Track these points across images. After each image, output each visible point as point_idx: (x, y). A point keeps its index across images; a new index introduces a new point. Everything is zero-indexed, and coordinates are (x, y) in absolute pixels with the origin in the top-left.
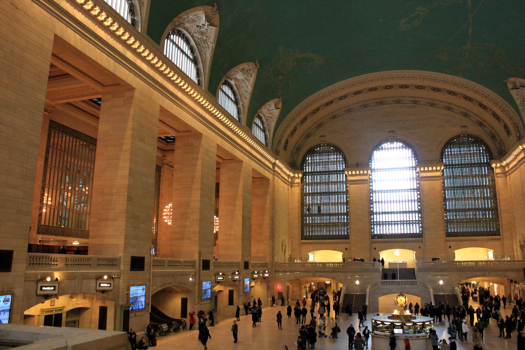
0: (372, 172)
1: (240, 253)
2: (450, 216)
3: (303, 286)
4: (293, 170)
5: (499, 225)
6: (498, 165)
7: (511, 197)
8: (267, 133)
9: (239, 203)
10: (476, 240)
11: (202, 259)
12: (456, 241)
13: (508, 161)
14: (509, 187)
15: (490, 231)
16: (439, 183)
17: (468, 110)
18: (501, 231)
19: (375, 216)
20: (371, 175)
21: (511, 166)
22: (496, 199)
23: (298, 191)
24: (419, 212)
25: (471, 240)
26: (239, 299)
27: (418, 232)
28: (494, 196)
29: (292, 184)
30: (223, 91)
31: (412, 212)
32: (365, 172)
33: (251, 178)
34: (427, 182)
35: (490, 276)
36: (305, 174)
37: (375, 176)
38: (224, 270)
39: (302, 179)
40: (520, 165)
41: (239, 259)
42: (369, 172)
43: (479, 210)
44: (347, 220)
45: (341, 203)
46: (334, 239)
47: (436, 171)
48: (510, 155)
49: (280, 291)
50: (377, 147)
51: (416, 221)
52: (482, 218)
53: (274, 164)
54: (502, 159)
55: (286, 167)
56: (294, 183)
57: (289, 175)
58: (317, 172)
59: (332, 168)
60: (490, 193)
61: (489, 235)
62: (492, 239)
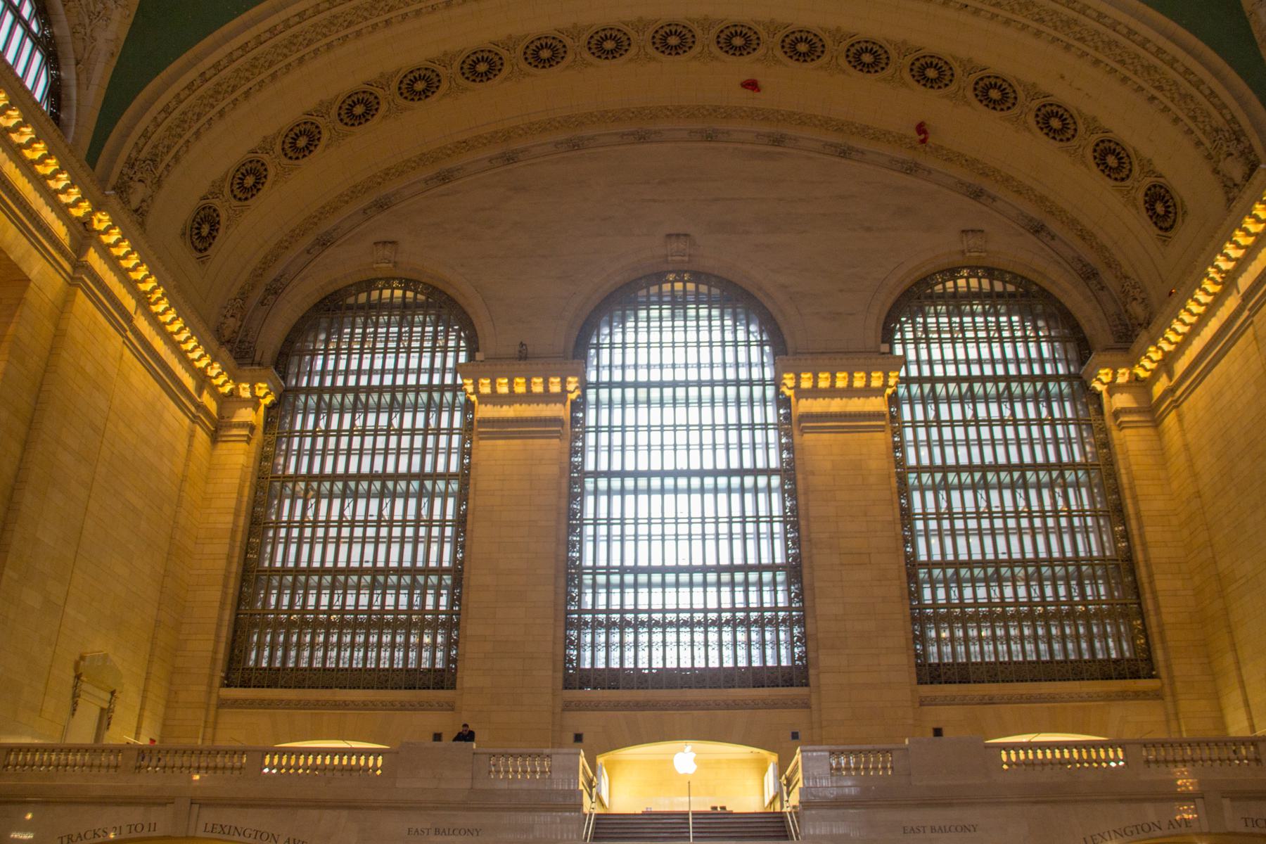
4: (224, 353)
5: (1145, 631)
6: (1123, 377)
7: (1198, 495)
10: (1052, 698)
12: (964, 701)
16: (881, 440)
18: (1159, 655)
20: (579, 405)
22: (1124, 520)
25: (1030, 699)
34: (825, 436)
39: (277, 414)
46: (383, 685)
47: (868, 391)
51: (775, 609)
54: (1143, 336)
62: (1123, 696)
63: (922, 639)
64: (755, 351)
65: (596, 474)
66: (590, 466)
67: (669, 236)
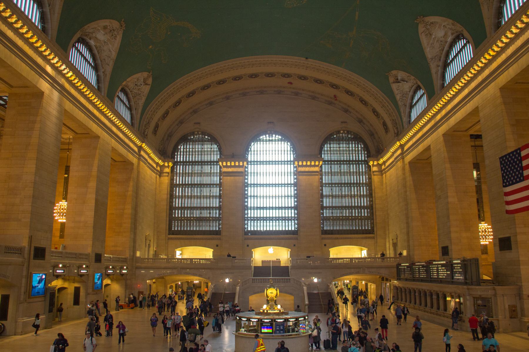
0: (248, 164)
1: (90, 243)
2: (327, 213)
3: (169, 286)
4: (162, 158)
5: (373, 223)
6: (375, 163)
7: (387, 195)
8: (134, 112)
9: (93, 184)
10: (351, 238)
11: (33, 246)
13: (385, 158)
14: (384, 186)
15: (365, 230)
16: (317, 178)
17: (349, 106)
18: (375, 229)
19: (249, 211)
21: (387, 164)
23: (167, 181)
24: (295, 208)
25: (346, 238)
26: (86, 298)
27: (293, 229)
28: (370, 195)
29: (160, 174)
30: (79, 51)
31: (288, 208)
32: (241, 164)
33: (110, 159)
35: (364, 273)
36: (176, 163)
37: (251, 168)
38: (67, 261)
39: (173, 169)
40: (396, 162)
41: (89, 250)
42: (245, 163)
43: (355, 207)
44: (219, 214)
45: (213, 197)
47: (315, 166)
48: (388, 151)
49: (141, 290)
50: (256, 138)
51: (291, 217)
52: (358, 216)
53: (140, 148)
54: (379, 156)
55: (154, 153)
56: (164, 173)
57: (158, 163)
58: (189, 162)
59: (206, 158)
60: (366, 192)
61: (363, 234)
62: (366, 238)
63: (323, 224)
64: (289, 152)
65: (251, 184)
66: (249, 183)
67: (268, 123)
